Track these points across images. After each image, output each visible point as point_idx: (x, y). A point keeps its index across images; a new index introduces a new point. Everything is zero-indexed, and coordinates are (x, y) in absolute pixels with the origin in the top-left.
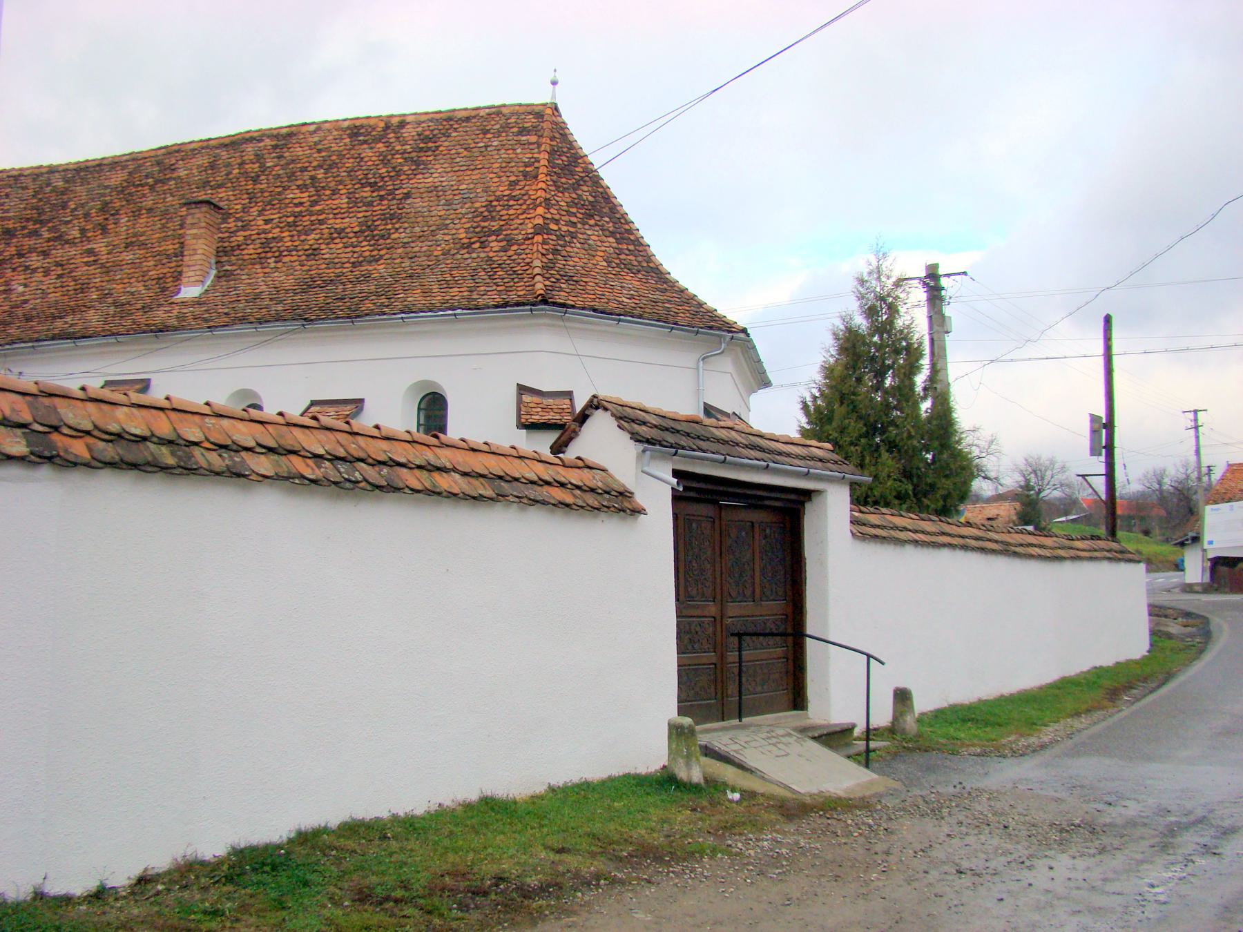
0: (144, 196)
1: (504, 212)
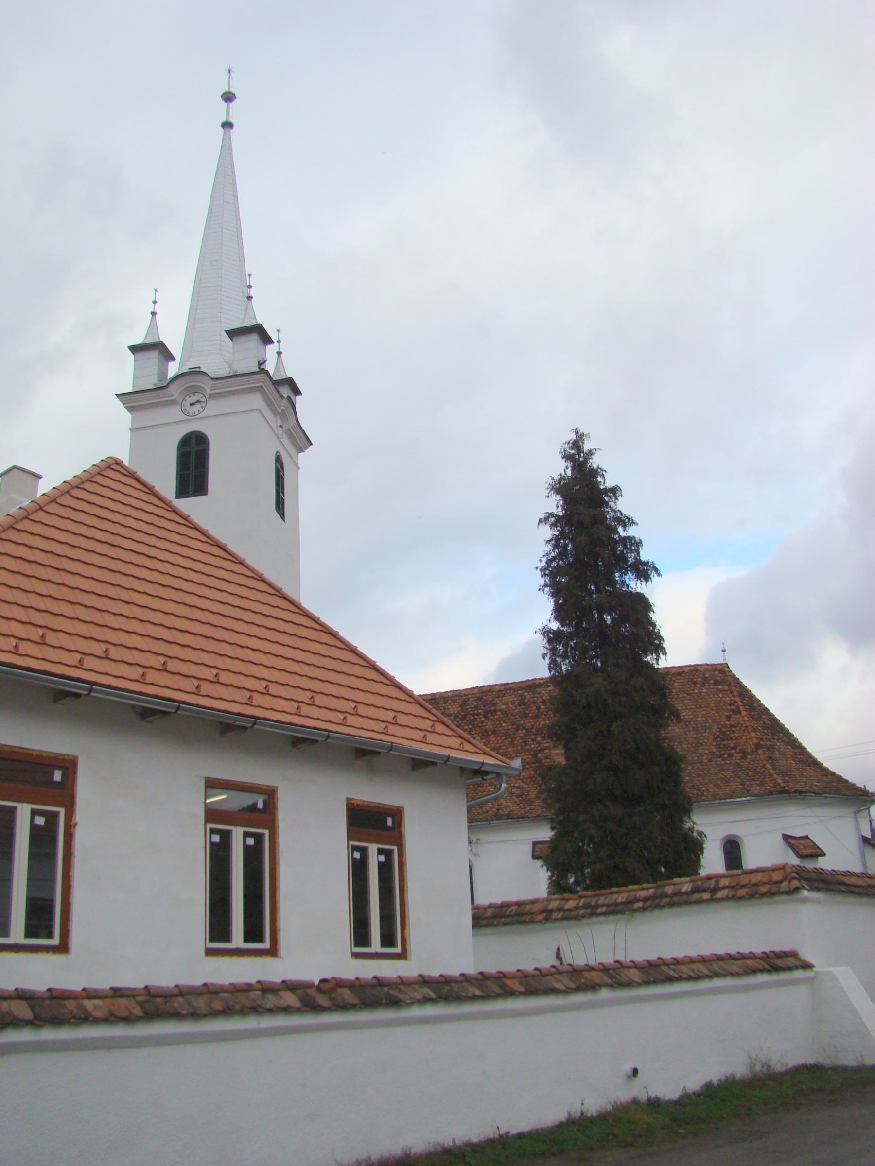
0: (482, 722)
1: (732, 735)
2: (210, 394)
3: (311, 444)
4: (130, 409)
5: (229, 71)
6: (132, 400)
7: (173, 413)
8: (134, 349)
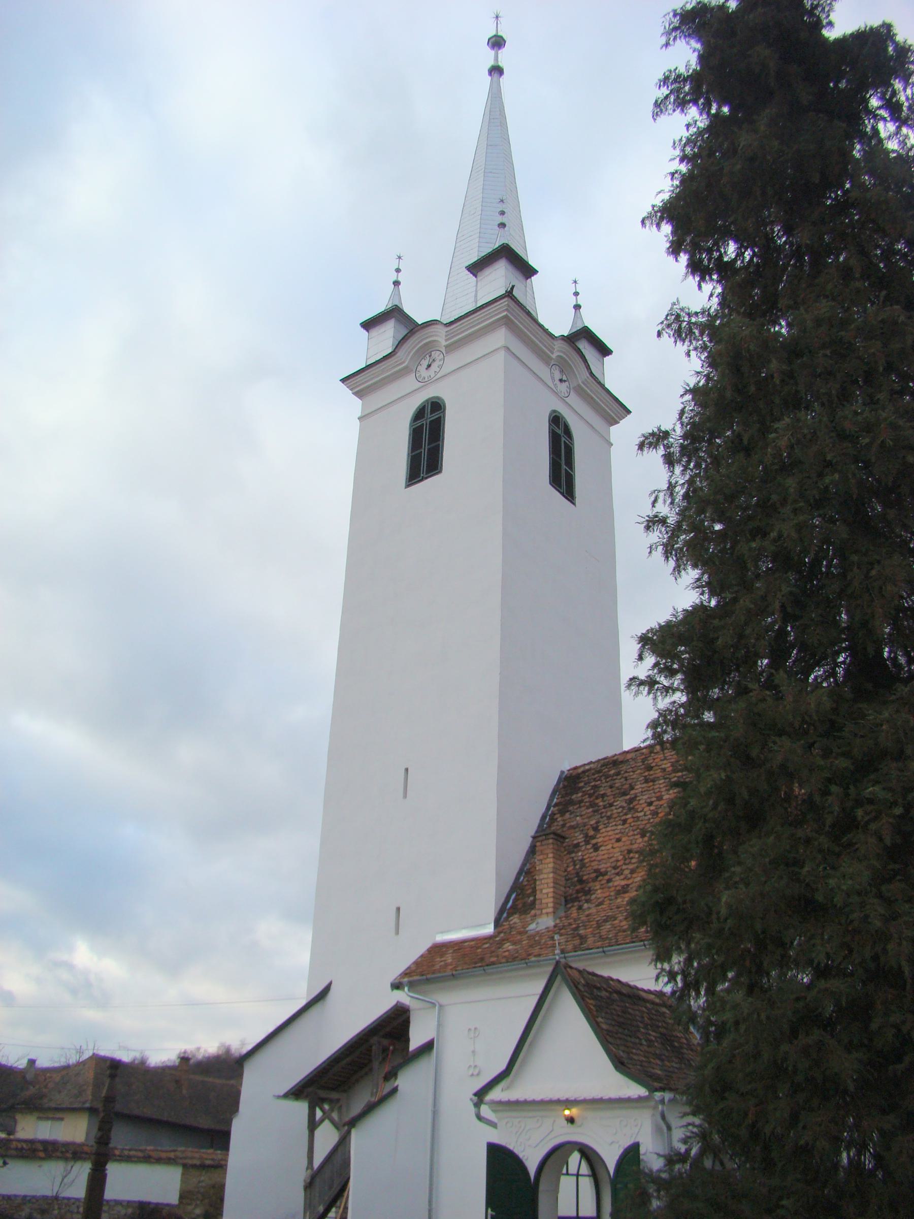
2: (446, 347)
3: (629, 412)
4: (359, 394)
5: (497, 17)
6: (359, 381)
7: (409, 383)
8: (368, 325)
